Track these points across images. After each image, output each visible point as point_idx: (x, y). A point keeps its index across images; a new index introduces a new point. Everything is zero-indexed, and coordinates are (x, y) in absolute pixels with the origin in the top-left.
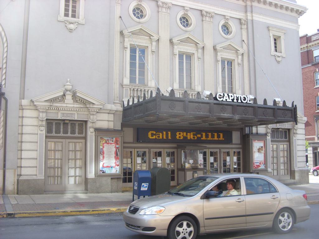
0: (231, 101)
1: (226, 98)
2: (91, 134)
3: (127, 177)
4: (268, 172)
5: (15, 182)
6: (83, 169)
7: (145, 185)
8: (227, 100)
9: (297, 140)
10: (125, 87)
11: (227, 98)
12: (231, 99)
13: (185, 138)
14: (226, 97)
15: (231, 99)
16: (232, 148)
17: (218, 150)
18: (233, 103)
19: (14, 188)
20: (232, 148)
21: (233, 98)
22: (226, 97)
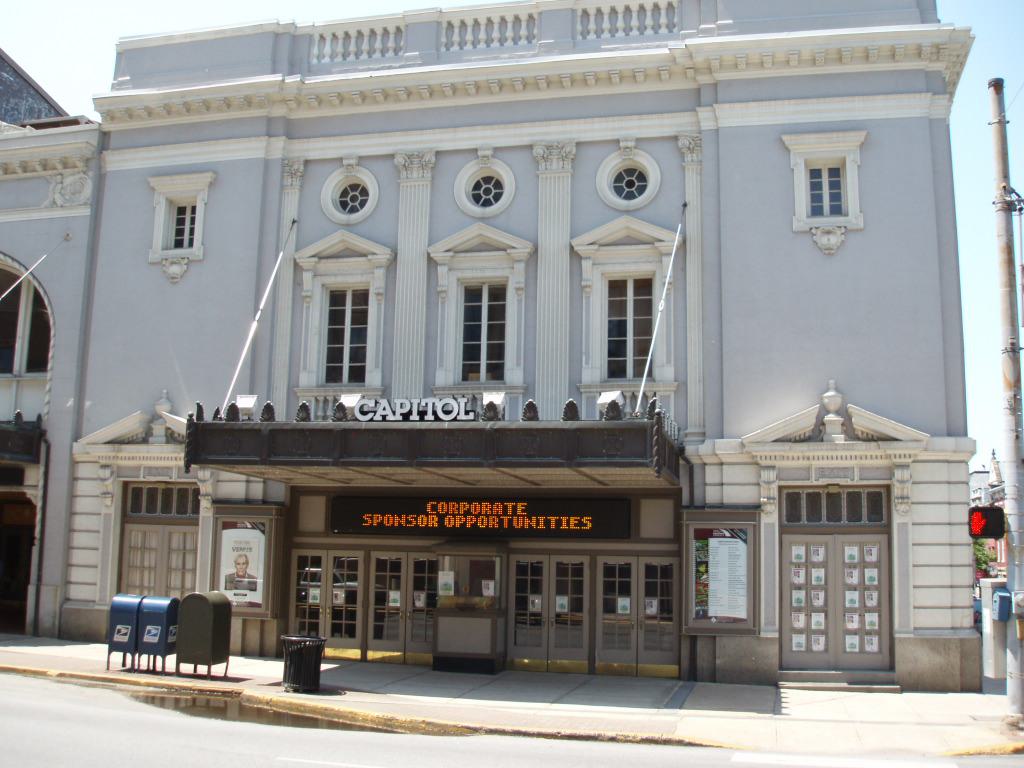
0: (401, 418)
1: (384, 413)
2: (206, 507)
3: (307, 620)
4: (759, 638)
5: (55, 613)
6: (786, 628)
7: (154, 632)
8: (388, 418)
9: (910, 526)
10: (586, 392)
11: (388, 412)
12: (401, 414)
13: (381, 524)
14: (384, 409)
15: (401, 414)
16: (638, 554)
17: (586, 560)
18: (406, 425)
19: (54, 624)
20: (638, 554)
21: (405, 410)
22: (384, 409)
